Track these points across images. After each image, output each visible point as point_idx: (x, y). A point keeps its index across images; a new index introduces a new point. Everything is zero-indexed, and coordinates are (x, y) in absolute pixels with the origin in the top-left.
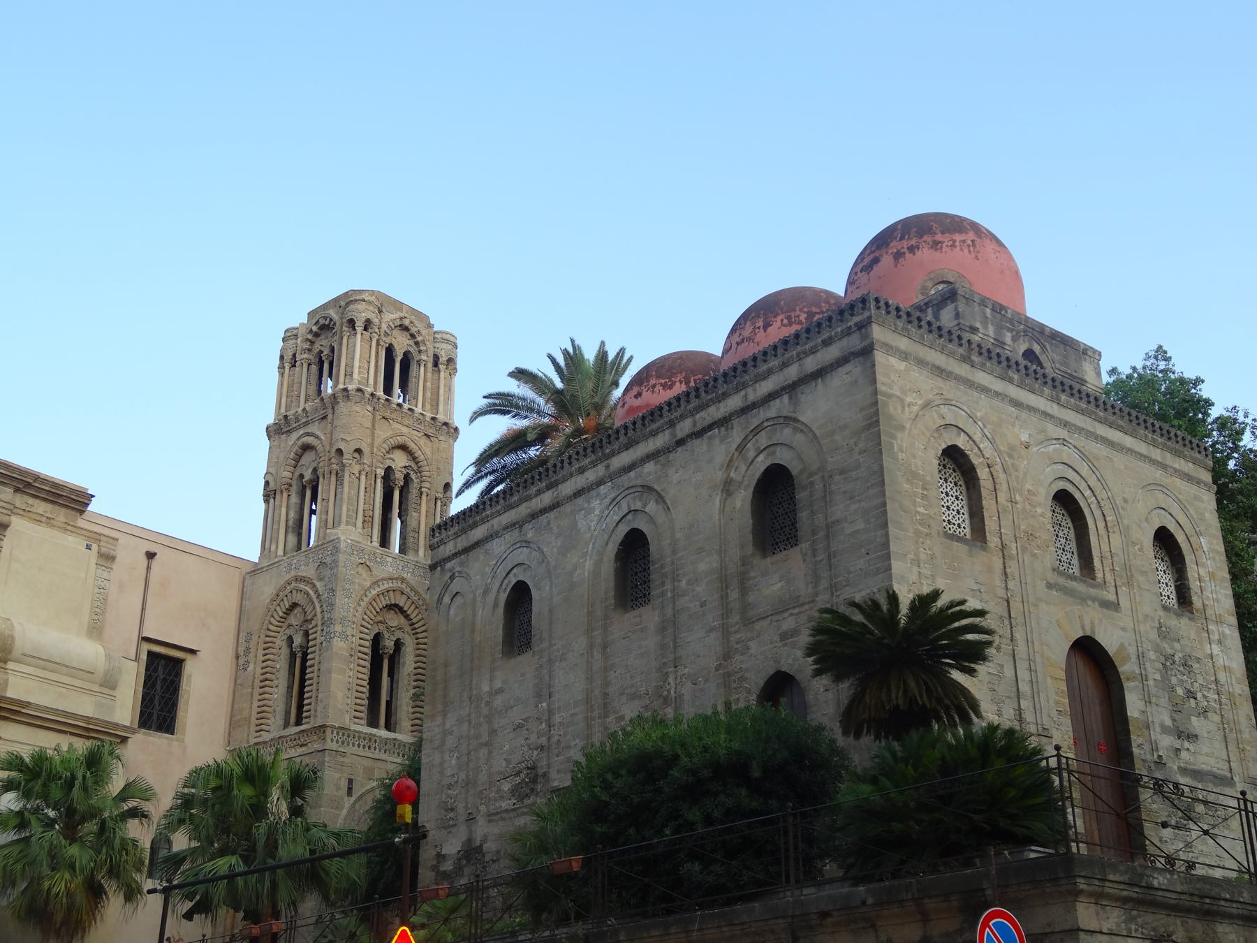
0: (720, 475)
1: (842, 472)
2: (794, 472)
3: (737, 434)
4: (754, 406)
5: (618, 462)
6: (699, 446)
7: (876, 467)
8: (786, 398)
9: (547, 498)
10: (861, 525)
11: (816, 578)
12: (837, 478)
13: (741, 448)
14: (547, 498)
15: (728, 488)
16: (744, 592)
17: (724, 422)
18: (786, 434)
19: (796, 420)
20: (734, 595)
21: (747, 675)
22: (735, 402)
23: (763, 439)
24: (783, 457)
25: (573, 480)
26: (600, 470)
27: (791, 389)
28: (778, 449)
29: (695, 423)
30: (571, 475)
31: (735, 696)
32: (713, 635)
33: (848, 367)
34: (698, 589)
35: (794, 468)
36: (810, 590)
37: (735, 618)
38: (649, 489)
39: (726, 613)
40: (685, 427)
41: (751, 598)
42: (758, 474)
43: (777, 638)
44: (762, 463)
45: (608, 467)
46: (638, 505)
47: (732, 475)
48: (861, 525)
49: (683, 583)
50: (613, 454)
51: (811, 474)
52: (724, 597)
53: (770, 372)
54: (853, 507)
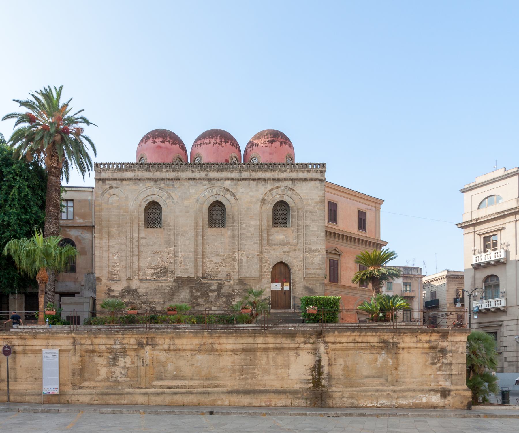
0: (261, 197)
1: (310, 212)
2: (290, 206)
3: (269, 186)
4: (278, 180)
5: (212, 175)
6: (253, 183)
7: (322, 215)
8: (290, 182)
9: (172, 175)
10: (316, 229)
11: (298, 238)
12: (308, 213)
13: (270, 191)
14: (172, 175)
15: (263, 201)
16: (268, 235)
17: (265, 180)
18: (290, 193)
19: (294, 190)
20: (265, 235)
21: (269, 260)
22: (268, 175)
23: (280, 191)
24: (286, 199)
25: (187, 173)
26: (203, 174)
27: (293, 180)
28: (285, 196)
29: (251, 175)
30: (187, 171)
31: (264, 265)
32: (256, 245)
33: (315, 182)
34: (250, 229)
35: (291, 204)
36: (294, 241)
37: (265, 242)
38: (228, 190)
39: (261, 239)
40: (245, 175)
41: (271, 238)
42: (276, 202)
43: (281, 252)
44: (278, 198)
45: (206, 175)
46: (222, 193)
47: (266, 198)
48: (316, 229)
49: (244, 226)
50: (210, 171)
51: (298, 209)
52: (261, 235)
53: (285, 171)
54: (313, 223)
